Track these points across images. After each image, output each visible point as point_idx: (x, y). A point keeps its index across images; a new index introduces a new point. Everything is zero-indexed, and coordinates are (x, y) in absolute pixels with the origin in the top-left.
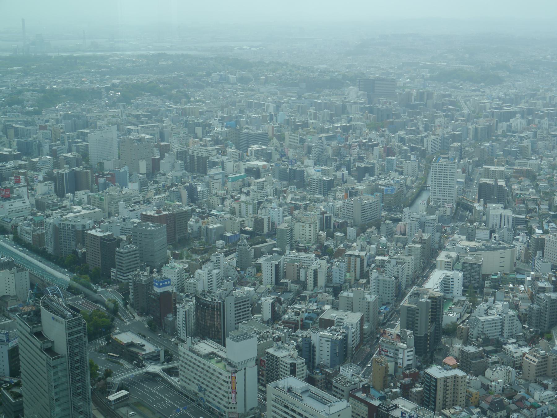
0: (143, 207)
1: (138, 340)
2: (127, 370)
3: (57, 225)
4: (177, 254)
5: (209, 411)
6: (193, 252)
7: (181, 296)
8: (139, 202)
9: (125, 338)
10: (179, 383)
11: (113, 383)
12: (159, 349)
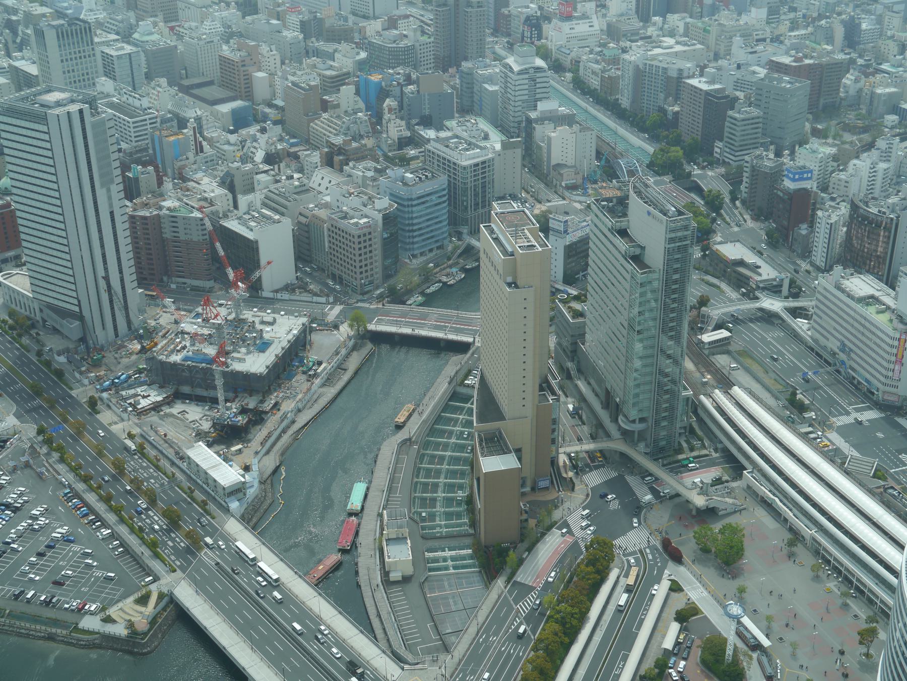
0: (770, 49)
1: (751, 258)
2: (731, 301)
3: (641, 67)
4: (819, 131)
5: (852, 384)
6: (844, 130)
7: (822, 199)
8: (764, 40)
9: (732, 251)
10: (809, 333)
11: (708, 316)
12: (783, 276)
